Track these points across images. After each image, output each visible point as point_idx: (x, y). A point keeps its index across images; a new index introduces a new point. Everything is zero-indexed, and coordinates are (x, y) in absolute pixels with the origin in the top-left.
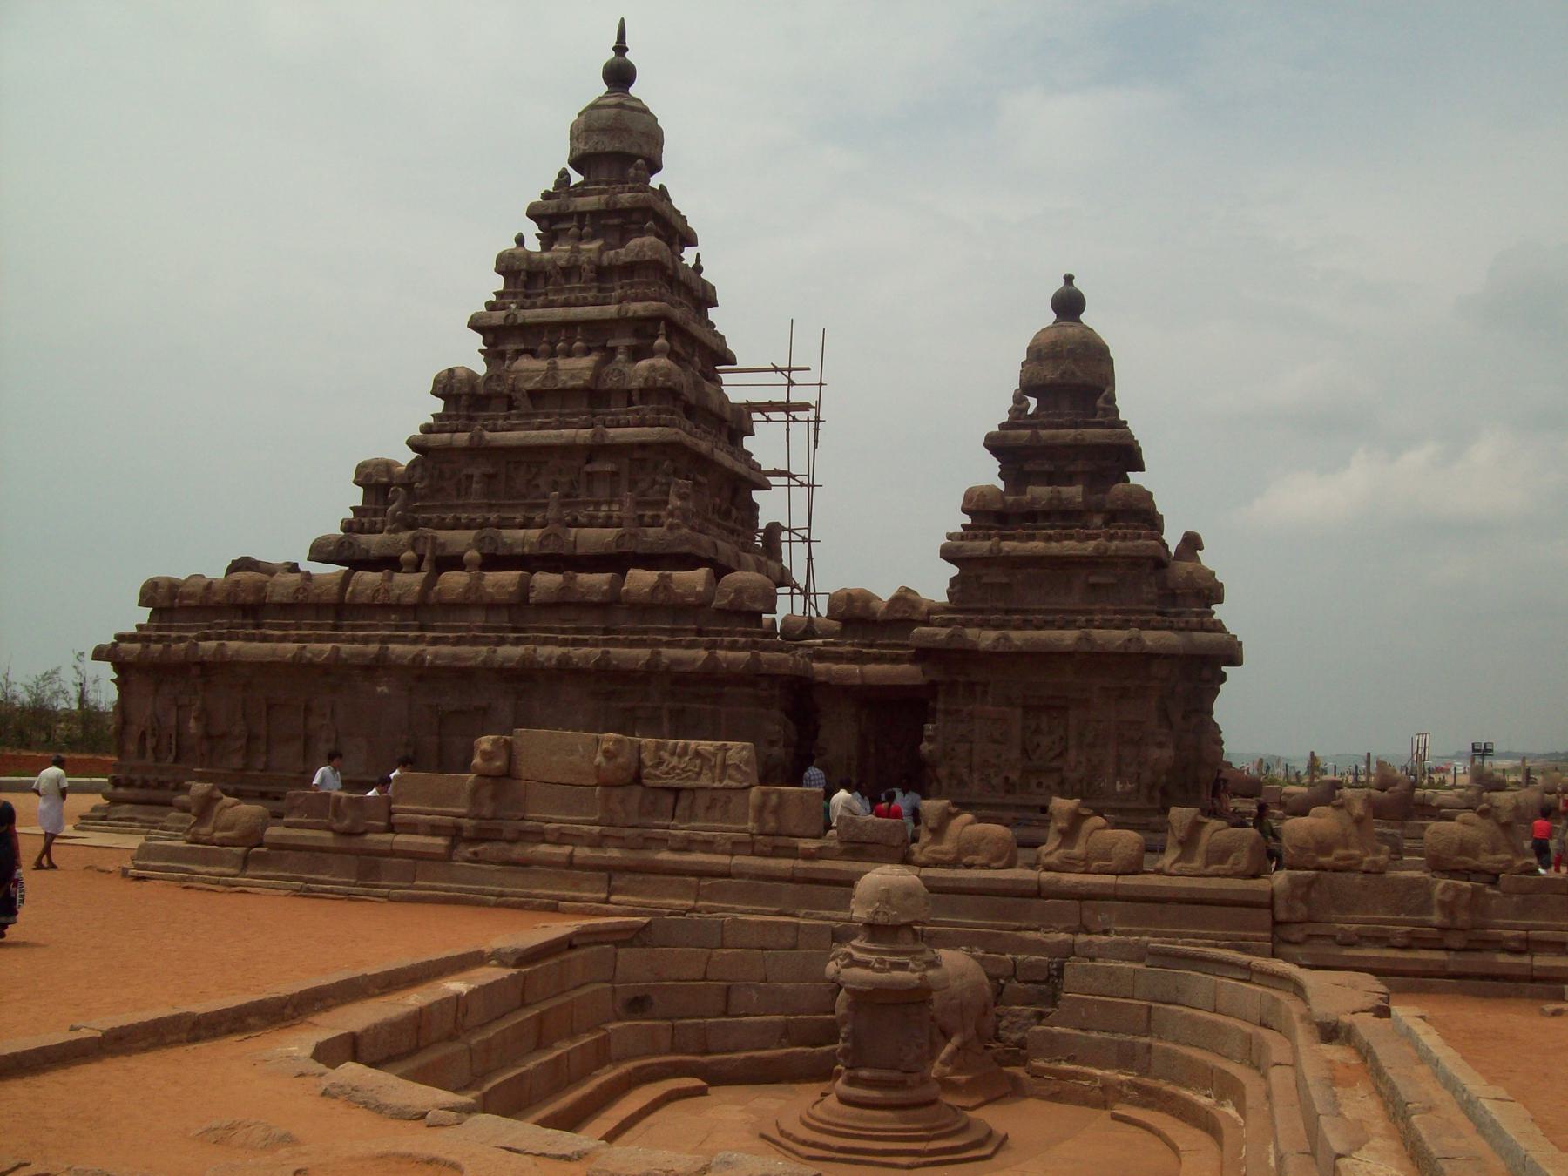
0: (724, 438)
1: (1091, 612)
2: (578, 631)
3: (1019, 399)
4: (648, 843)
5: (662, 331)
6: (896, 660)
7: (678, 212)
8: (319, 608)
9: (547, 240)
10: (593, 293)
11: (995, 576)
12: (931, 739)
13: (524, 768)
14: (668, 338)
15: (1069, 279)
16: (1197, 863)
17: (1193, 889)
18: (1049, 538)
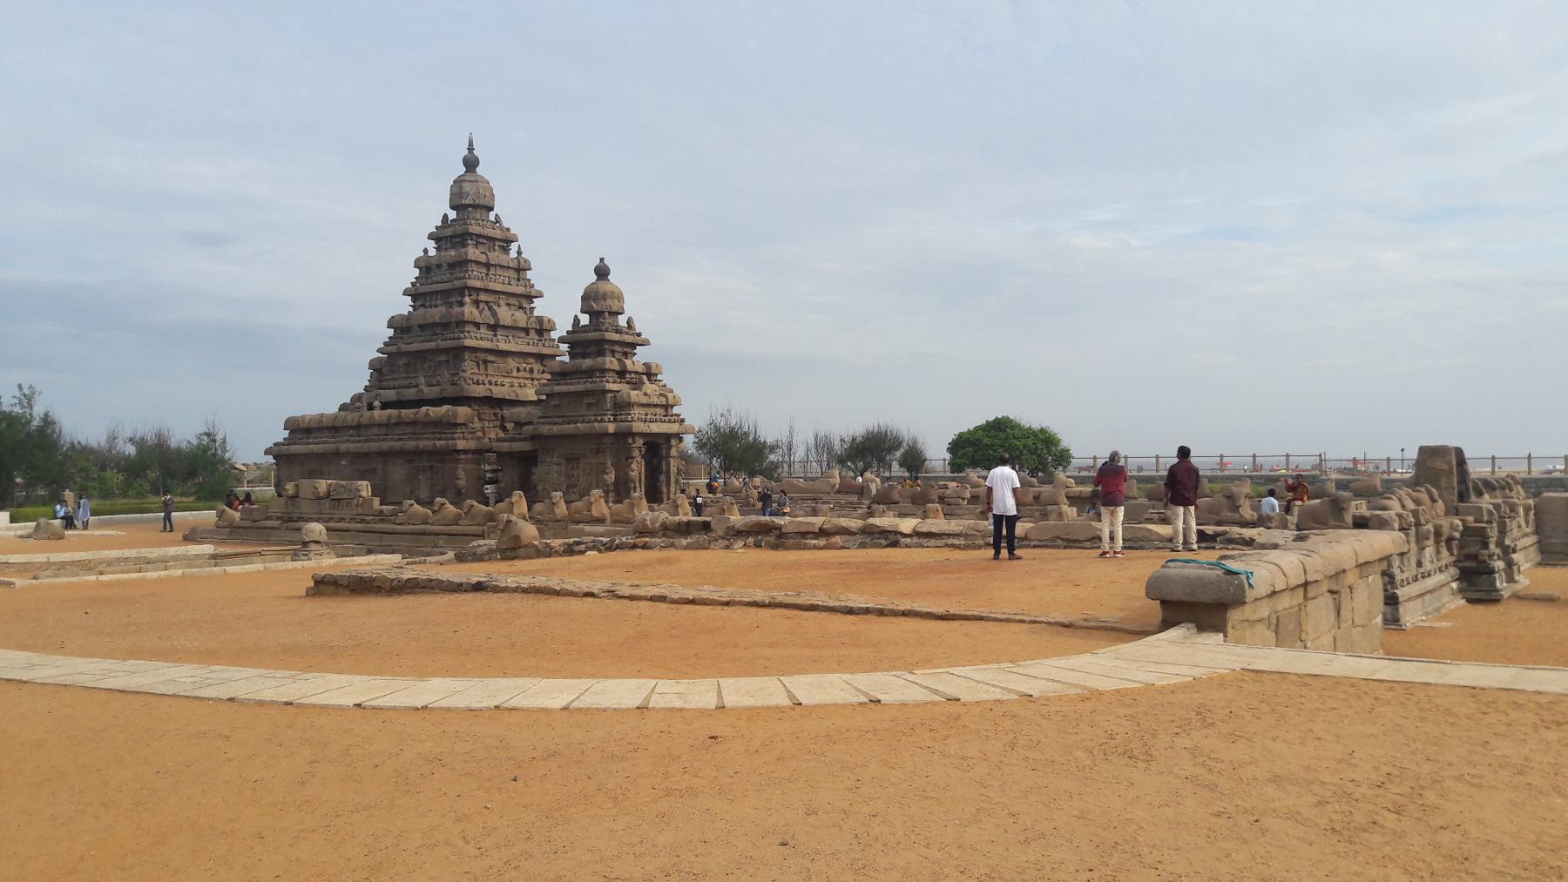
0: (533, 334)
1: (585, 416)
2: (403, 434)
3: (576, 320)
4: (330, 520)
5: (467, 294)
6: (525, 440)
7: (501, 228)
8: (329, 429)
9: (438, 249)
10: (448, 275)
11: (555, 402)
12: (534, 474)
13: (301, 495)
14: (470, 295)
15: (602, 260)
16: (466, 522)
17: (462, 531)
18: (571, 384)
